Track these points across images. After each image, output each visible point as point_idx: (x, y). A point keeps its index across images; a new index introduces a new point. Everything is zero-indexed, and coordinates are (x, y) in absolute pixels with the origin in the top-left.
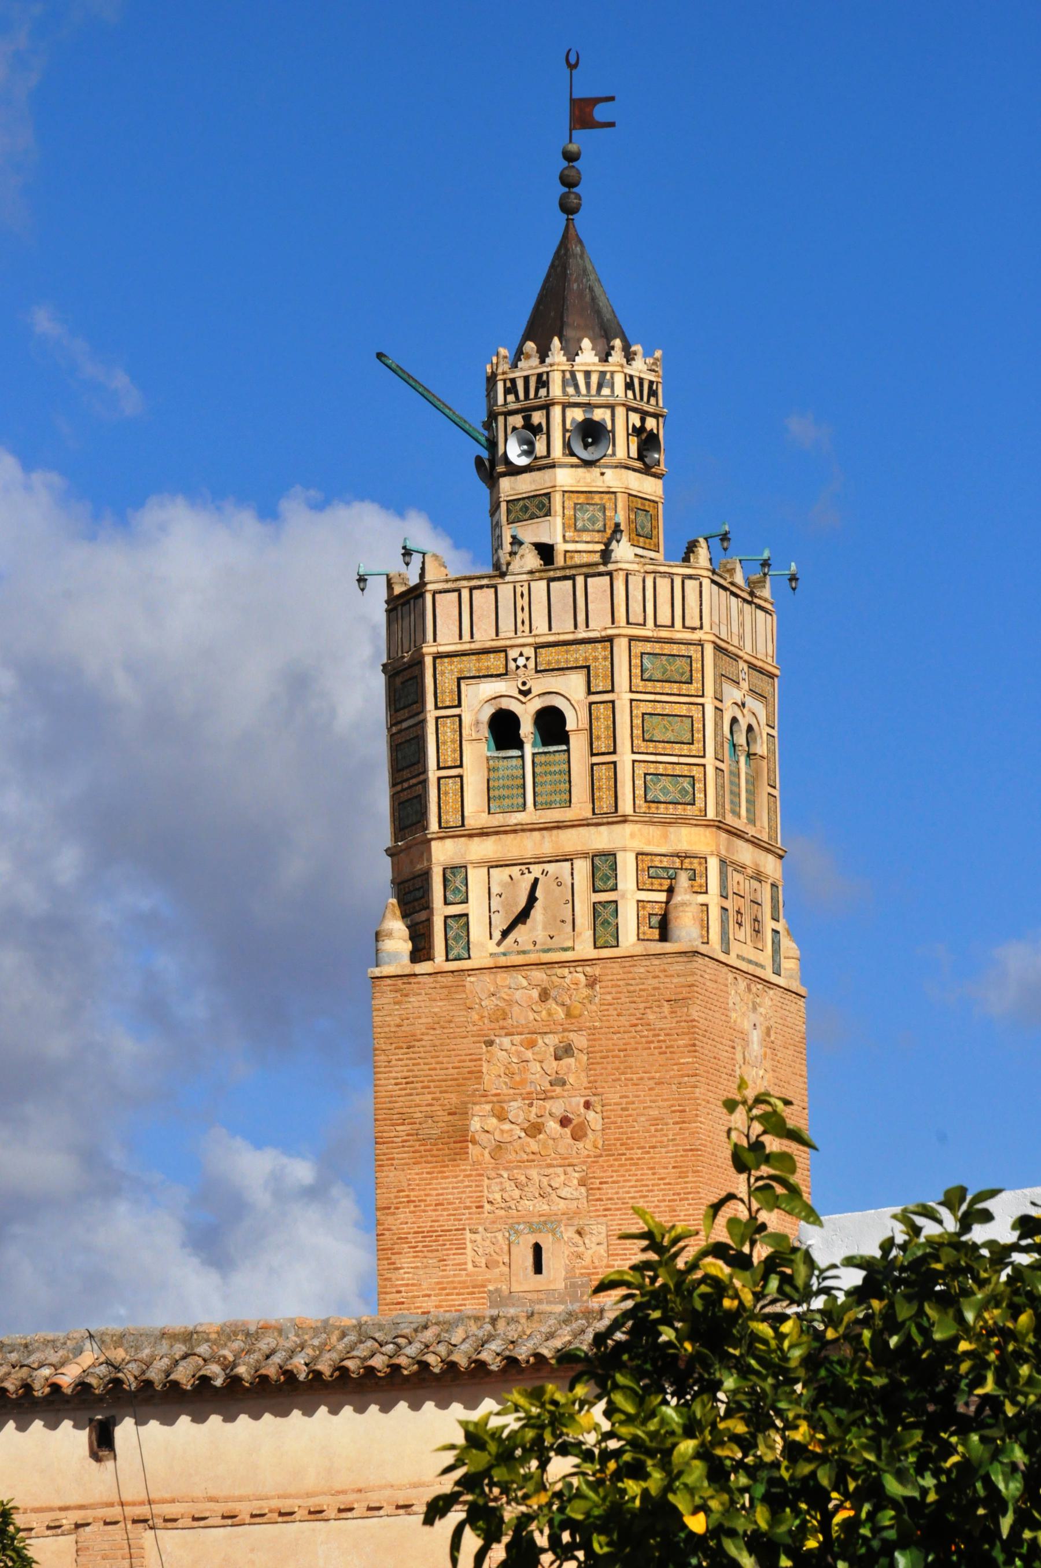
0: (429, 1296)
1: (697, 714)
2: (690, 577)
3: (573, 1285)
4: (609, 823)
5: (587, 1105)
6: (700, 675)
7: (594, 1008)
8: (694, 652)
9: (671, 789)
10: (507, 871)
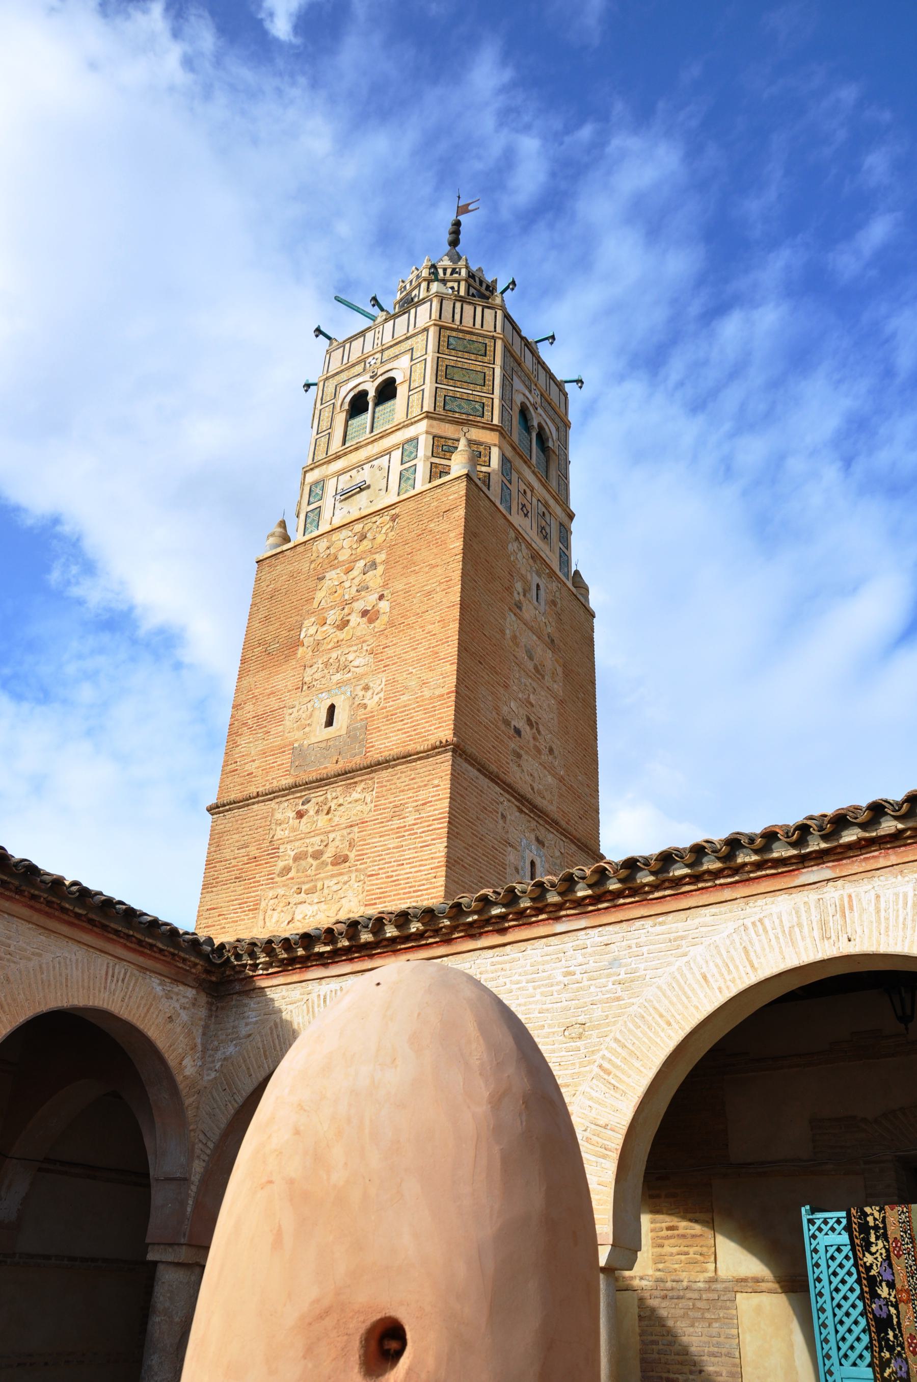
0: (254, 761)
1: (489, 373)
2: (489, 308)
3: (355, 729)
4: (416, 422)
5: (381, 597)
6: (492, 353)
7: (393, 533)
8: (487, 341)
9: (465, 406)
10: (349, 474)
